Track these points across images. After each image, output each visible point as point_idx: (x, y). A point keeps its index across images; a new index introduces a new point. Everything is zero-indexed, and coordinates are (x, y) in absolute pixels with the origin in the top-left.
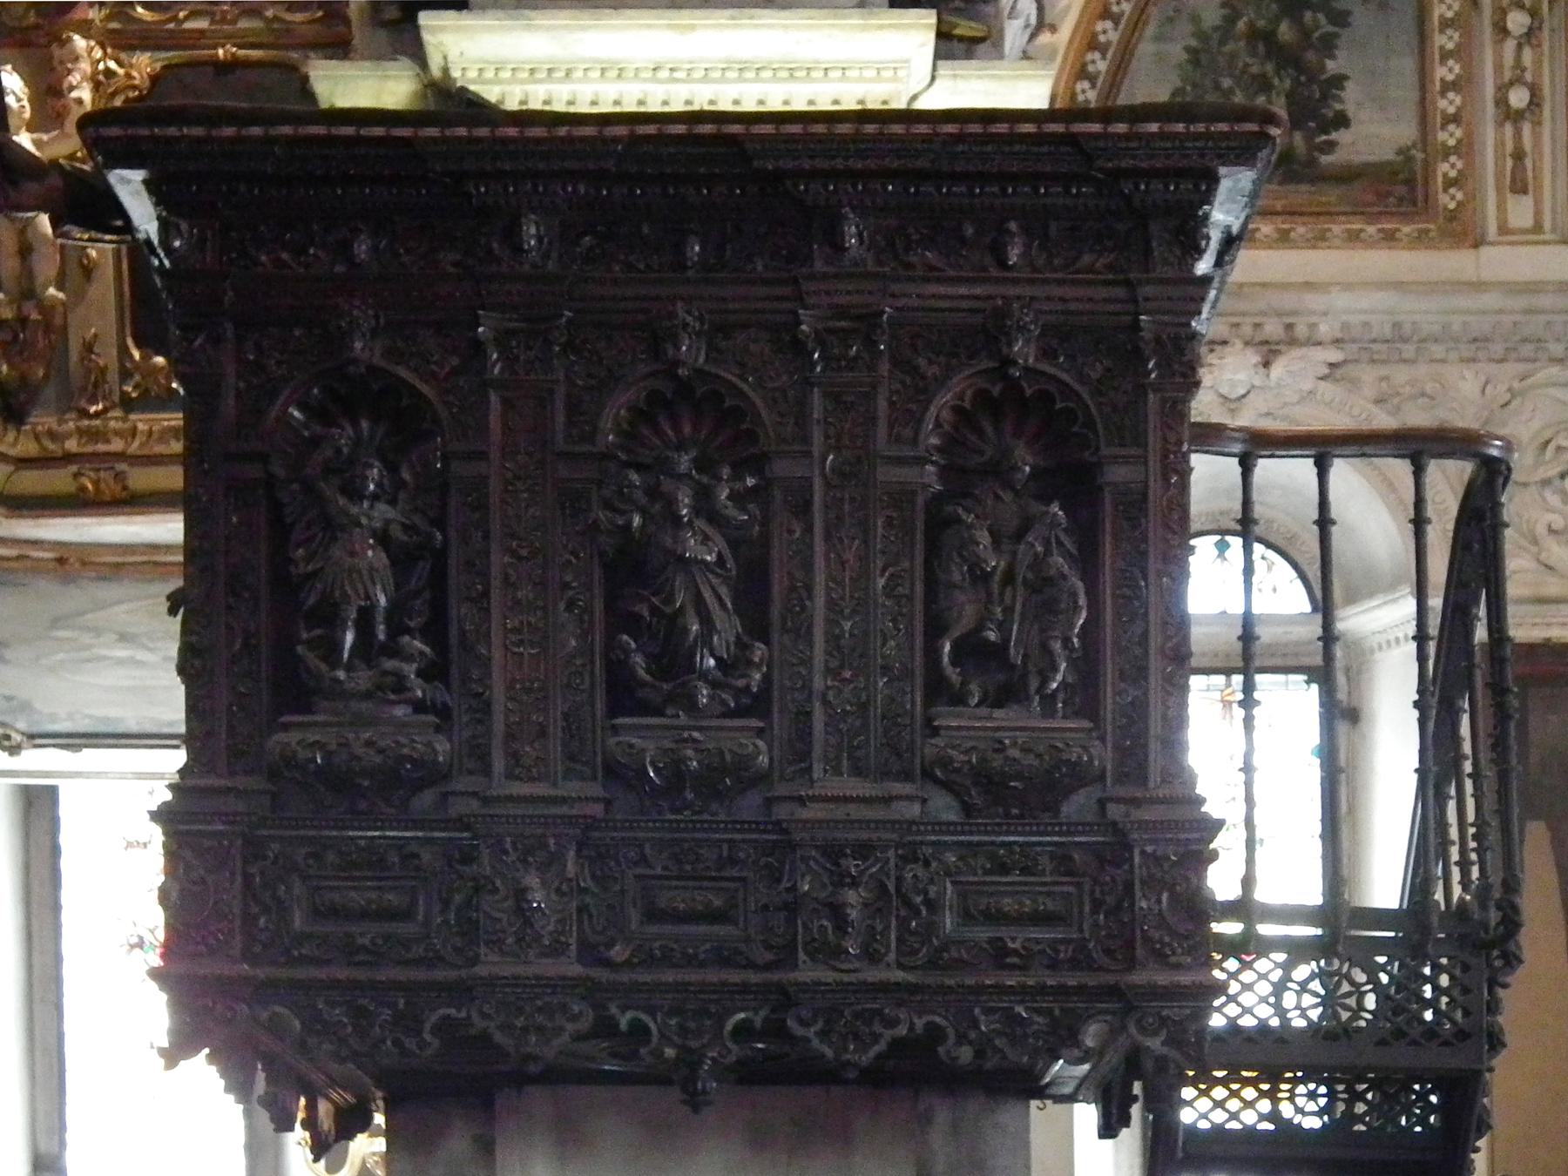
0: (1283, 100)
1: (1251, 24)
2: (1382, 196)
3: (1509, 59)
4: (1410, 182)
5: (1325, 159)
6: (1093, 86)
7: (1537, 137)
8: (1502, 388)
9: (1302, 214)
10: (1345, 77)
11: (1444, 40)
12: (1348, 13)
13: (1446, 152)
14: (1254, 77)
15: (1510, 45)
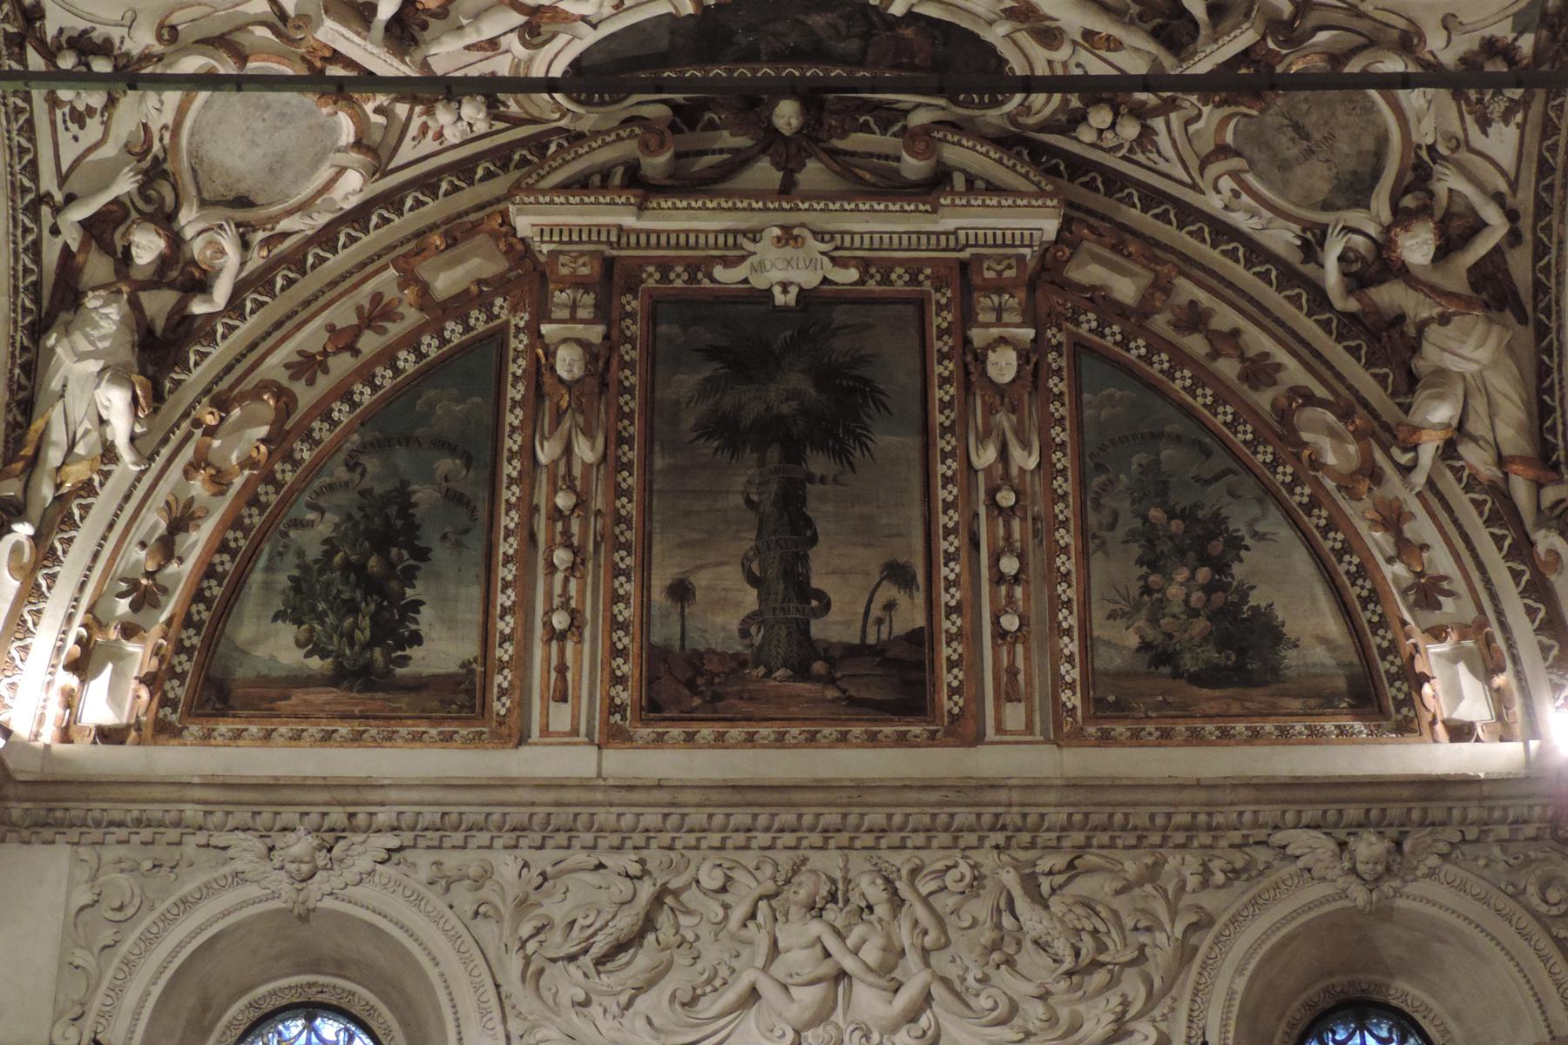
0: (367, 620)
1: (346, 559)
2: (445, 704)
3: (558, 590)
4: (470, 693)
5: (399, 671)
6: (208, 609)
7: (578, 654)
8: (535, 872)
9: (375, 718)
10: (422, 603)
11: (507, 573)
12: (429, 550)
13: (502, 666)
14: (344, 601)
15: (559, 577)
